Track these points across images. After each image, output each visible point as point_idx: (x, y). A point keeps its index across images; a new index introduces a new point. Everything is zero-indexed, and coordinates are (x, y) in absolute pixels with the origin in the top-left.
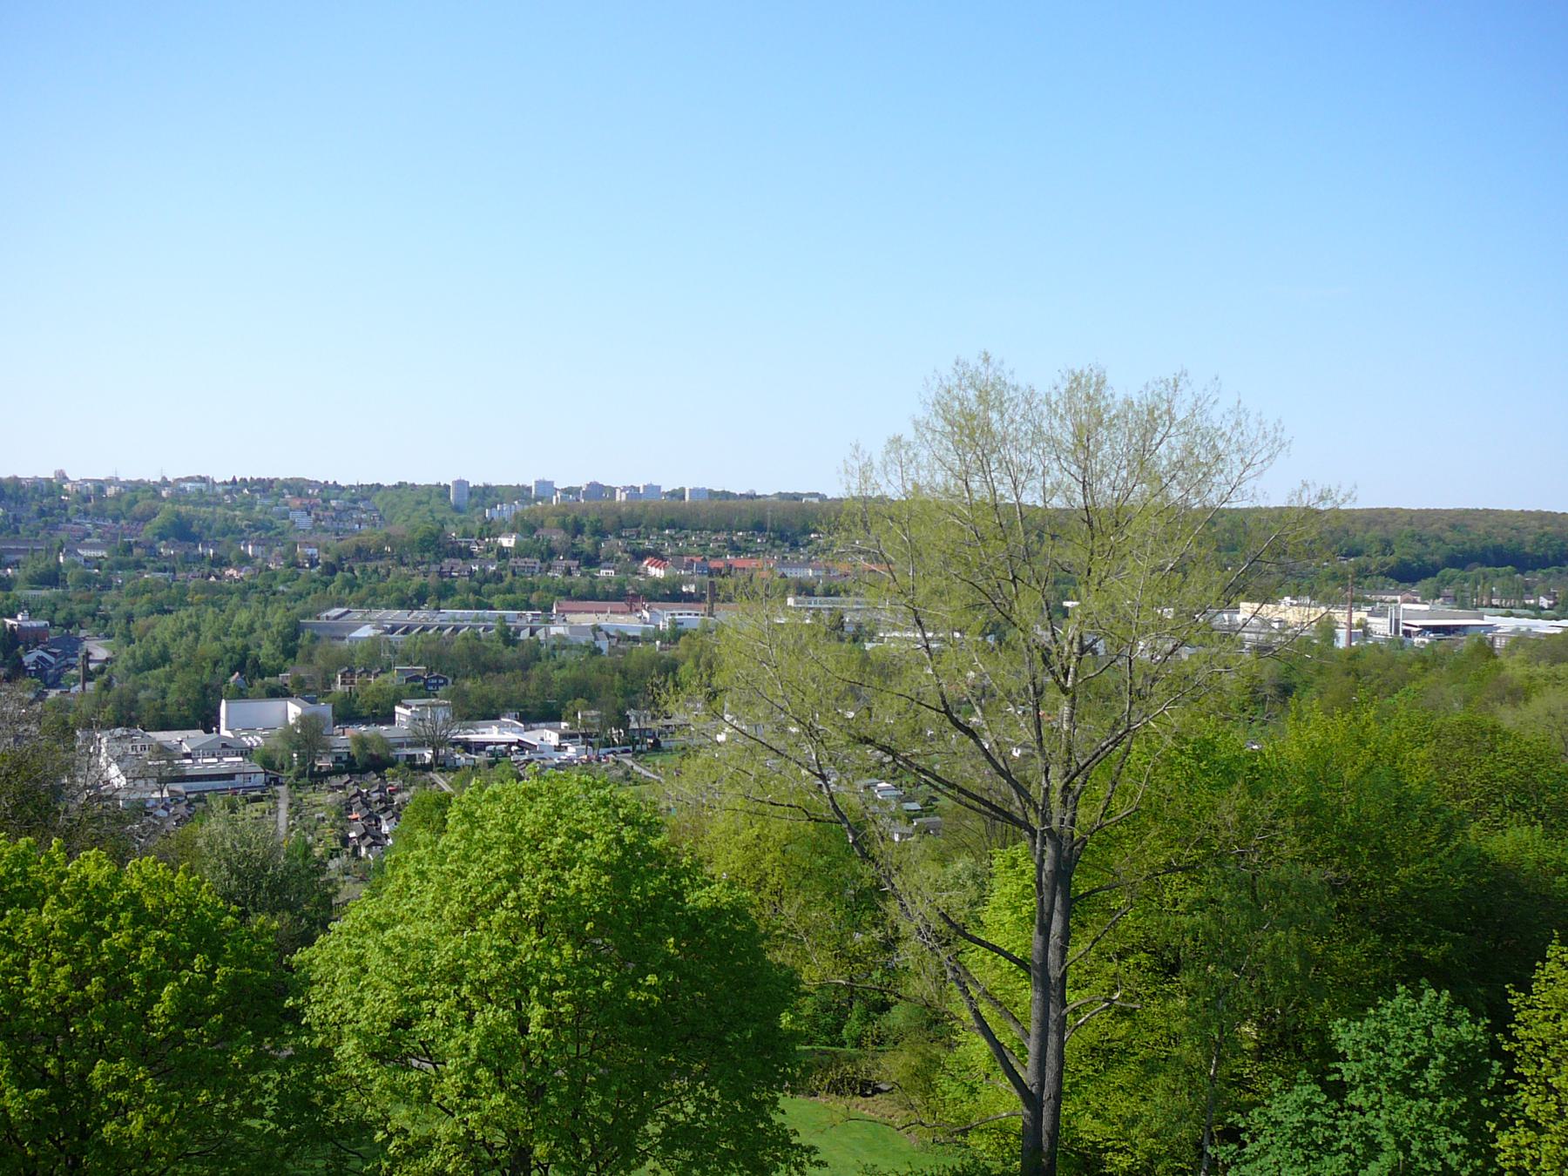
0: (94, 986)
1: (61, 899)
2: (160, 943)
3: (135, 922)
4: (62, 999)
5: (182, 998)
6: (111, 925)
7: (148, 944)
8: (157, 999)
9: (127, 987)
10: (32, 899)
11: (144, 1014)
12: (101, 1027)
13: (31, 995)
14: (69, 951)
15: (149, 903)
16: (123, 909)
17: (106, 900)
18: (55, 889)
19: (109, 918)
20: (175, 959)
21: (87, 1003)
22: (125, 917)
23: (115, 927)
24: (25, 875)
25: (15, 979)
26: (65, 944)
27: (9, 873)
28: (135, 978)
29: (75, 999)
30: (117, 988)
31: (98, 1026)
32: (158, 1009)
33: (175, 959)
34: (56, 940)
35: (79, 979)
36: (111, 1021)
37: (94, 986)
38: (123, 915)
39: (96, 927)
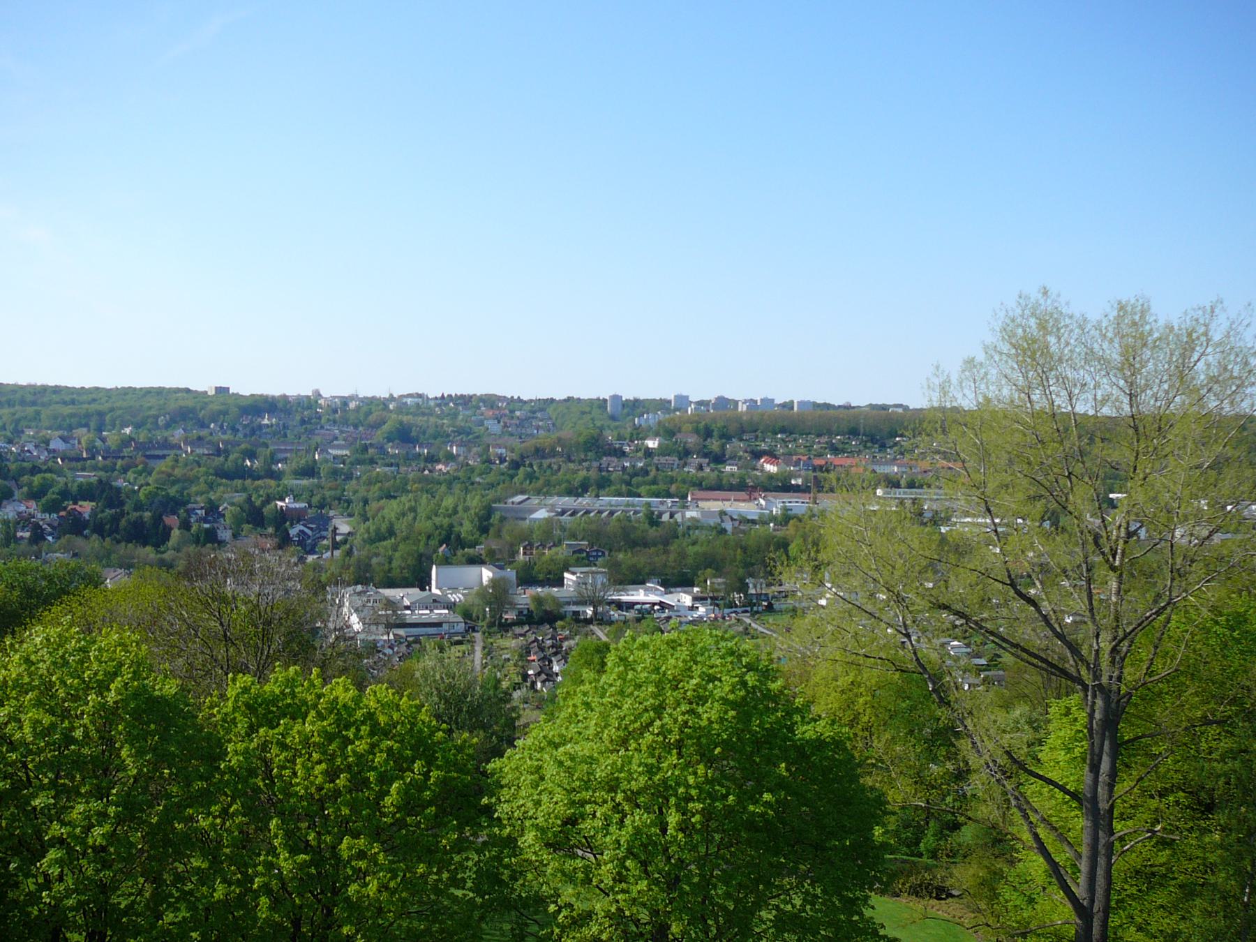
1: (319, 715)
2: (390, 749)
3: (372, 733)
4: (320, 789)
5: (405, 793)
7: (381, 751)
8: (388, 793)
9: (366, 782)
10: (298, 713)
12: (348, 812)
13: (298, 784)
14: (325, 753)
15: (382, 719)
16: (363, 723)
17: (350, 715)
18: (315, 706)
19: (353, 730)
20: (401, 764)
21: (337, 793)
22: (365, 729)
23: (358, 737)
25: (287, 772)
26: (321, 748)
27: (282, 693)
28: (372, 776)
29: (329, 790)
30: (359, 783)
31: (345, 811)
32: (388, 800)
33: (401, 764)
35: (332, 775)
36: (355, 807)
37: (342, 781)
38: (363, 728)
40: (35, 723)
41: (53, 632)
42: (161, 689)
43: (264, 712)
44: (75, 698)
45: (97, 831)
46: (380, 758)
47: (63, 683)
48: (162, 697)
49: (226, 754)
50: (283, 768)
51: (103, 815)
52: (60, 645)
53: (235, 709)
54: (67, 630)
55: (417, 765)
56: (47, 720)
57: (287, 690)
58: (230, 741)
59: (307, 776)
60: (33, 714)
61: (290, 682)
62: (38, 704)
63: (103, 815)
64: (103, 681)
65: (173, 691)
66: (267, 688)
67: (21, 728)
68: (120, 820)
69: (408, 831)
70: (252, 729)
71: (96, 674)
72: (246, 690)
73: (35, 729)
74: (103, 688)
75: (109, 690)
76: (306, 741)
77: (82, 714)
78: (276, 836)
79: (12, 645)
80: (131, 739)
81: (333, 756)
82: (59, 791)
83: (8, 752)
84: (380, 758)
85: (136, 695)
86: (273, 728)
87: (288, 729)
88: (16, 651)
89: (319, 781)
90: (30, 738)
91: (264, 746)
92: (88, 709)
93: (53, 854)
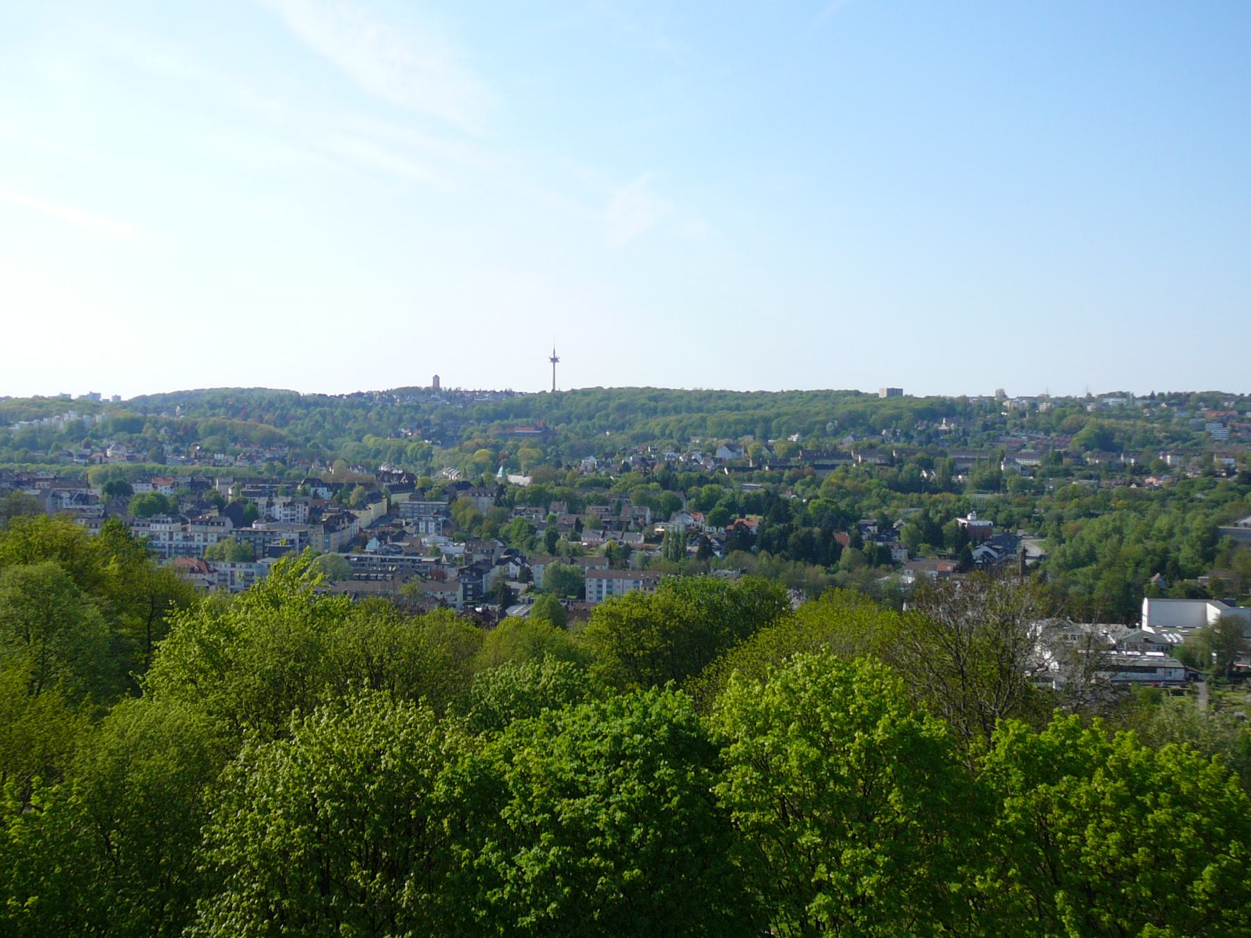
0: (1141, 855)
1: (1108, 774)
2: (1197, 825)
3: (1173, 803)
4: (1112, 862)
5: (1222, 878)
6: (1152, 801)
7: (1187, 825)
8: (1198, 876)
9: (1168, 860)
10: (1081, 770)
11: (1183, 888)
12: (1149, 893)
13: (1088, 854)
14: (1117, 819)
15: (1185, 787)
16: (1161, 788)
17: (1145, 779)
18: (1102, 763)
19: (1150, 795)
20: (1210, 844)
21: (1134, 870)
22: (1164, 797)
23: (1157, 805)
24: (1074, 747)
25: (1073, 838)
26: (1114, 812)
27: (1063, 743)
28: (1178, 853)
29: (1125, 864)
30: (1161, 861)
31: (1146, 892)
32: (1198, 886)
33: (1210, 844)
34: (1106, 808)
35: (1127, 847)
36: (1158, 889)
37: (1141, 855)
38: (1162, 795)
39: (1137, 802)
40: (802, 756)
41: (810, 658)
42: (928, 730)
43: (1041, 766)
44: (840, 734)
45: (865, 880)
46: (1185, 834)
47: (827, 715)
48: (931, 739)
49: (1002, 808)
50: (1066, 833)
51: (871, 862)
52: (820, 674)
53: (1008, 759)
54: (825, 658)
55: (1234, 845)
56: (814, 753)
57: (1069, 742)
58: (1005, 795)
59: (1098, 845)
60: (796, 748)
61: (1073, 732)
62: (803, 732)
63: (871, 862)
64: (868, 717)
65: (943, 732)
66: (1043, 736)
67: (786, 760)
69: (1222, 926)
70: (1029, 784)
72: (1020, 738)
73: (801, 761)
74: (867, 725)
75: (875, 727)
76: (1095, 804)
78: (1063, 912)
79: (772, 671)
81: (1129, 825)
82: (830, 831)
84: (1185, 834)
85: (902, 734)
86: (1053, 785)
87: (1072, 788)
88: (777, 678)
89: (1113, 852)
90: (796, 772)
91: (1045, 806)
92: (856, 745)
93: (821, 899)
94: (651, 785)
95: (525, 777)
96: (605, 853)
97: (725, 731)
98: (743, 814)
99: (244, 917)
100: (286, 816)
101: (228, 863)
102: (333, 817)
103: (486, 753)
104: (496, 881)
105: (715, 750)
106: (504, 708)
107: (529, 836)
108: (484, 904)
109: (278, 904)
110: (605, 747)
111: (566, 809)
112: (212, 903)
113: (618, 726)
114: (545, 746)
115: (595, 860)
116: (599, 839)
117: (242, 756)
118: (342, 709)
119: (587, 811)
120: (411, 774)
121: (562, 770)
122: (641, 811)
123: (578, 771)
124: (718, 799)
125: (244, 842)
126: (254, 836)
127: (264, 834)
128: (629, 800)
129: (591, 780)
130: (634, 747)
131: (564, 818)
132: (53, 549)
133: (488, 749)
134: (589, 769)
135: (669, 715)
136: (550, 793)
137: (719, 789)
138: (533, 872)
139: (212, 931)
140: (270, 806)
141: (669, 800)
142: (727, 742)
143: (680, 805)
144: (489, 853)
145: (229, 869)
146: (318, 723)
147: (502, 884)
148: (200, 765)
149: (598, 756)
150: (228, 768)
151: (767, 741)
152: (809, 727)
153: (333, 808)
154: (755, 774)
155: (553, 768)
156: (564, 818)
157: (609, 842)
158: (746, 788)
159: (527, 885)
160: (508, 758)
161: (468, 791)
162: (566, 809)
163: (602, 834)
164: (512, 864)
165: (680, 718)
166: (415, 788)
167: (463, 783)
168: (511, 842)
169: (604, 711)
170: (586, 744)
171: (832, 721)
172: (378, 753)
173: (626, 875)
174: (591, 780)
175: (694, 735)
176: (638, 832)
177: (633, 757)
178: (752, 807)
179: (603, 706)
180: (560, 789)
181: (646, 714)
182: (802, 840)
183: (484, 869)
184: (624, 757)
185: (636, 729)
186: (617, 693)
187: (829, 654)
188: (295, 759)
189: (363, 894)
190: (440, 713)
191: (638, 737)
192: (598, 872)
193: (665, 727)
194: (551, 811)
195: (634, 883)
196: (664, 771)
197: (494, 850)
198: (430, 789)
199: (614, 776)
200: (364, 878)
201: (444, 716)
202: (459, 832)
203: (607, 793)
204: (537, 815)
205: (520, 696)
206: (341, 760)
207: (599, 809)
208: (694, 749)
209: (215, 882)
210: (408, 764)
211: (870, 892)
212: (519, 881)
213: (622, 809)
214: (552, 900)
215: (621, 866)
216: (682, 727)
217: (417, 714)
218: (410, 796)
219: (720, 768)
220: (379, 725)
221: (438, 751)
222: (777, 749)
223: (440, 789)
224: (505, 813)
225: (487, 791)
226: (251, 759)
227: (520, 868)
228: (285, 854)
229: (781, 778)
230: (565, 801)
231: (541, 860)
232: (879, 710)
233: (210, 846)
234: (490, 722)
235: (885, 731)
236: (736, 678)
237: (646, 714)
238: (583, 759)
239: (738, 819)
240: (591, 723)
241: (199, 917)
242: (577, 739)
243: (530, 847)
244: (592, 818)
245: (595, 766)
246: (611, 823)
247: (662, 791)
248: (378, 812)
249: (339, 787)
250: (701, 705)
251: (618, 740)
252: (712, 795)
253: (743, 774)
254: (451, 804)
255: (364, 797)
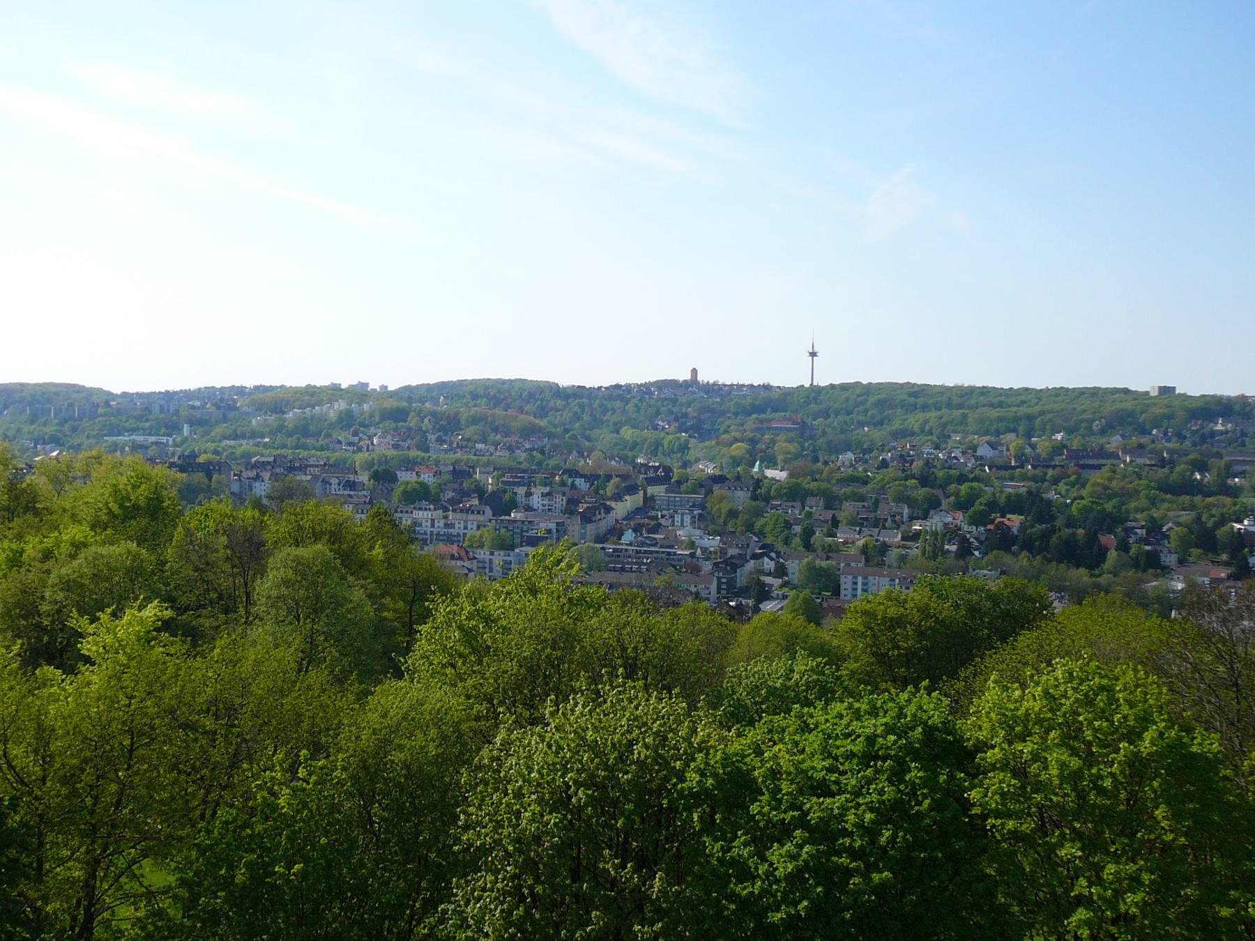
40: (1063, 765)
52: (1082, 681)
56: (1075, 763)
60: (1056, 756)
62: (1064, 743)
63: (1135, 880)
67: (1046, 768)
68: (1154, 888)
71: (1125, 717)
74: (1133, 736)
77: (1113, 762)
79: (1032, 676)
80: (1164, 795)
82: (1091, 844)
83: (1033, 792)
88: (1037, 684)
90: (1056, 781)
92: (1120, 757)
93: (1081, 914)
94: (902, 787)
95: (774, 774)
96: (854, 854)
97: (983, 735)
98: (999, 821)
99: (496, 898)
100: (540, 801)
101: (483, 844)
102: (586, 805)
103: (735, 747)
104: (746, 875)
105: (971, 755)
106: (756, 703)
107: (783, 833)
108: (733, 897)
109: (531, 888)
110: (858, 747)
111: (816, 808)
112: (467, 882)
113: (871, 725)
114: (796, 744)
115: (844, 860)
116: (847, 841)
117: (498, 740)
118: (597, 698)
119: (836, 811)
120: (662, 765)
121: (813, 768)
122: (890, 813)
123: (831, 770)
124: (974, 805)
125: (499, 825)
126: (510, 819)
127: (518, 817)
128: (878, 802)
129: (843, 779)
130: (888, 747)
131: (813, 817)
132: (323, 533)
133: (739, 743)
134: (841, 768)
135: (925, 717)
136: (801, 791)
137: (974, 795)
138: (785, 869)
139: (469, 910)
140: (524, 791)
141: (919, 803)
142: (983, 746)
143: (931, 809)
144: (741, 849)
145: (484, 851)
146: (572, 710)
147: (754, 878)
148: (460, 746)
149: (850, 756)
150: (485, 752)
151: (1027, 748)
152: (1071, 734)
153: (587, 795)
154: (1013, 782)
155: (804, 766)
156: (813, 817)
157: (858, 844)
158: (1003, 795)
159: (777, 881)
160: (759, 752)
161: (720, 782)
162: (816, 808)
163: (850, 835)
164: (764, 859)
165: (936, 720)
166: (667, 779)
167: (715, 775)
168: (763, 839)
169: (858, 710)
170: (838, 743)
171: (1096, 730)
172: (631, 743)
173: (876, 877)
174: (843, 779)
175: (950, 738)
176: (887, 834)
177: (884, 759)
178: (1009, 815)
179: (856, 705)
180: (812, 787)
181: (901, 715)
182: (1062, 853)
183: (734, 862)
184: (876, 758)
185: (889, 729)
186: (872, 693)
187: (1091, 660)
188: (550, 746)
189: (614, 882)
190: (692, 706)
191: (892, 738)
192: (848, 873)
193: (920, 729)
194: (799, 808)
195: (883, 884)
196: (915, 773)
197: (746, 844)
198: (682, 779)
199: (863, 777)
200: (616, 867)
201: (696, 709)
202: (709, 825)
203: (858, 794)
204: (785, 812)
205: (772, 692)
206: (593, 747)
207: (848, 809)
208: (948, 752)
209: (472, 862)
210: (661, 756)
211: (1134, 909)
212: (770, 874)
213: (872, 810)
214: (803, 898)
215: (871, 868)
216: (937, 729)
217: (669, 706)
218: (661, 787)
219: (977, 773)
220: (631, 715)
221: (691, 744)
222: (1036, 757)
223: (693, 778)
224: (754, 809)
225: (736, 787)
226: (506, 744)
227: (772, 864)
228: (537, 839)
229: (1039, 787)
230: (814, 799)
231: (793, 857)
232: (1145, 720)
233: (466, 827)
234: (741, 716)
235: (1153, 743)
236: (995, 682)
237: (901, 715)
238: (836, 758)
239: (993, 826)
240: (844, 722)
241: (456, 895)
242: (830, 737)
243: (782, 845)
244: (841, 818)
245: (847, 766)
246: (860, 825)
247: (915, 794)
248: (630, 801)
249: (593, 776)
250: (958, 708)
251: (871, 740)
252: (968, 800)
253: (999, 781)
254: (698, 797)
255: (618, 785)
